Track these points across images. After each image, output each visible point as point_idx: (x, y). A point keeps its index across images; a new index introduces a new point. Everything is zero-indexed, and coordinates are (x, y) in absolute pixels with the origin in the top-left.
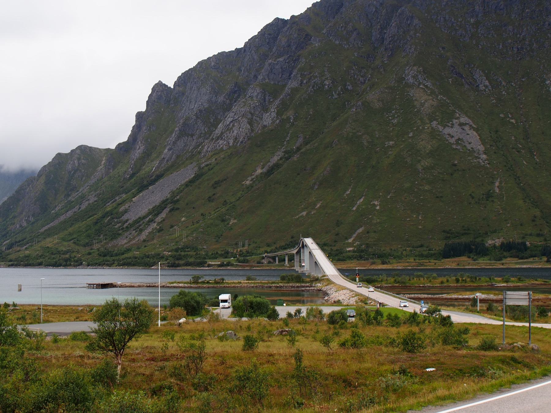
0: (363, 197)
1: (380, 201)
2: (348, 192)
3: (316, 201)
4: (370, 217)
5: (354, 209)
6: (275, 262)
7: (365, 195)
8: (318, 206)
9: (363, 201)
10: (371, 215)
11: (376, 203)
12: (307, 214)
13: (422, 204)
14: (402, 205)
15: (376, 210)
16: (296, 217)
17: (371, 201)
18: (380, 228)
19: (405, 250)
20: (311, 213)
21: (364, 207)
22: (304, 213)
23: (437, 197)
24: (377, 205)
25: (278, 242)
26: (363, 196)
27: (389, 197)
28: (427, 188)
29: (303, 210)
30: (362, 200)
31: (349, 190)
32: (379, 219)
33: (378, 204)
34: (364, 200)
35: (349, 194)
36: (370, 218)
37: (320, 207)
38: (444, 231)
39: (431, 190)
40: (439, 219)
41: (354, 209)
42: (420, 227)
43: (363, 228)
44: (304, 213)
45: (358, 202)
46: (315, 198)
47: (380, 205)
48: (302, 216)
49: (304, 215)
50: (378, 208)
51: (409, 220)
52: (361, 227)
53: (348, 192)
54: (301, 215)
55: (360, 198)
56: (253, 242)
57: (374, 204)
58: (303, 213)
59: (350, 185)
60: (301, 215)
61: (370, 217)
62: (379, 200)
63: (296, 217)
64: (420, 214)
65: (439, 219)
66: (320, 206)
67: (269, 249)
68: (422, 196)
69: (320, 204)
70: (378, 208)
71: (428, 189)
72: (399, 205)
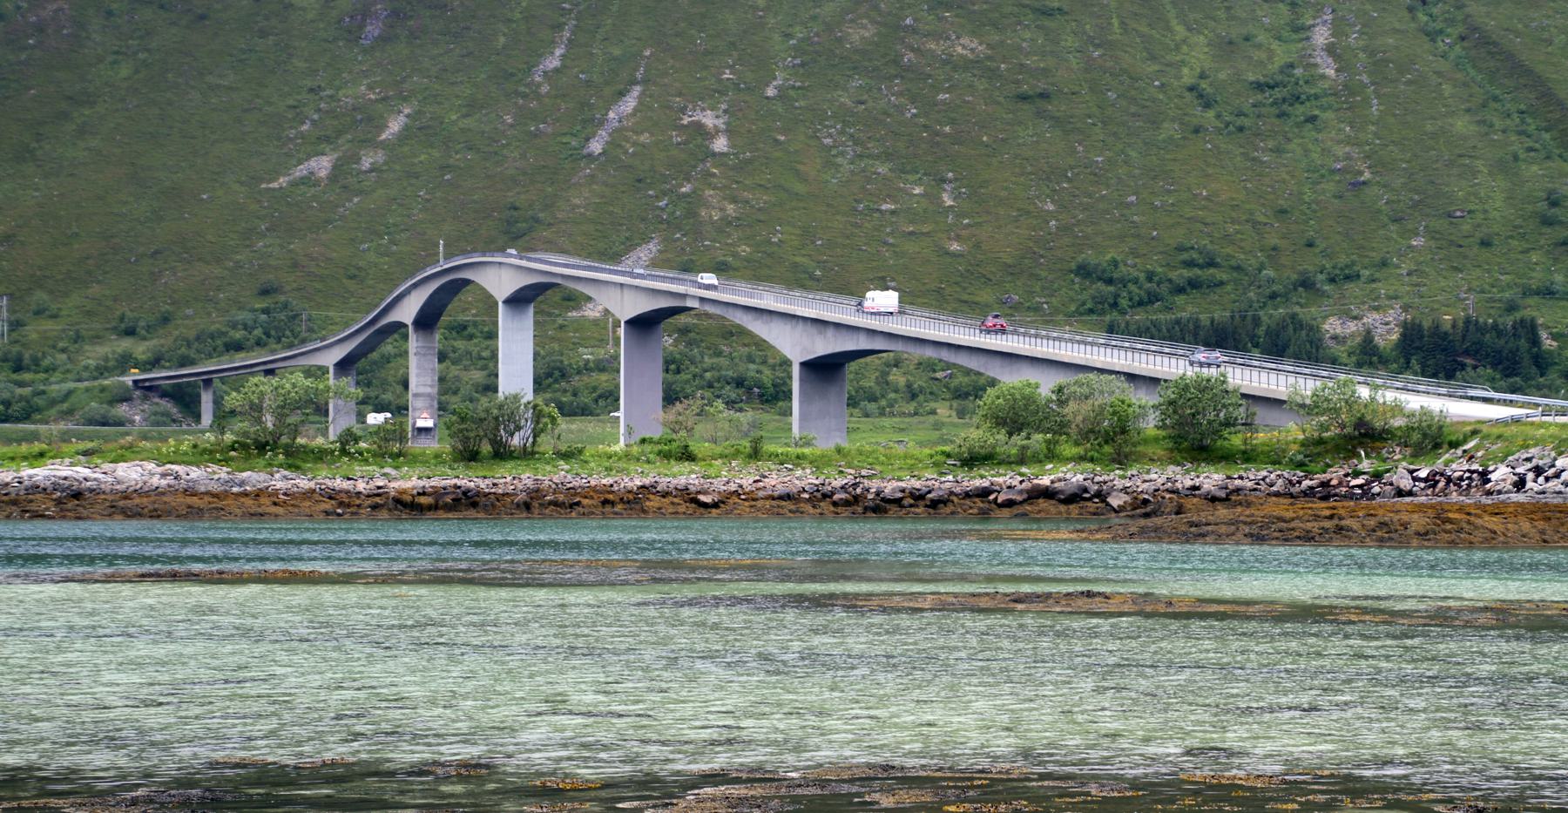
0: (637, 91)
1: (725, 111)
2: (553, 63)
3: (376, 100)
4: (684, 190)
5: (596, 147)
6: (190, 420)
7: (645, 81)
8: (395, 126)
9: (636, 110)
10: (689, 181)
11: (709, 120)
12: (337, 168)
13: (947, 129)
14: (842, 132)
15: (714, 154)
16: (275, 185)
17: (683, 110)
18: (744, 250)
19: (896, 366)
20: (358, 161)
21: (645, 138)
22: (322, 165)
23: (1024, 98)
24: (717, 131)
25: (189, 312)
26: (634, 82)
27: (770, 92)
28: (966, 46)
29: (317, 144)
30: (629, 104)
31: (558, 52)
32: (734, 200)
33: (720, 123)
34: (641, 102)
35: (556, 70)
36: (685, 195)
37: (405, 136)
38: (1084, 271)
39: (989, 58)
40: (1051, 207)
41: (596, 147)
42: (955, 247)
43: (651, 246)
44: (322, 165)
45: (611, 115)
46: (370, 88)
47: (730, 132)
48: (309, 180)
49: (323, 174)
50: (720, 144)
51: (893, 212)
52: (646, 239)
53: (553, 63)
54: (300, 171)
55: (622, 94)
56: (38, 313)
57: (698, 126)
58: (313, 163)
59: (559, 27)
60: (300, 171)
61: (684, 190)
62: (724, 106)
63: (275, 185)
64: (944, 180)
65: (1051, 207)
66: (406, 128)
67: (141, 350)
68: (948, 91)
69: (402, 119)
70: (720, 144)
71: (971, 56)
72: (830, 136)
